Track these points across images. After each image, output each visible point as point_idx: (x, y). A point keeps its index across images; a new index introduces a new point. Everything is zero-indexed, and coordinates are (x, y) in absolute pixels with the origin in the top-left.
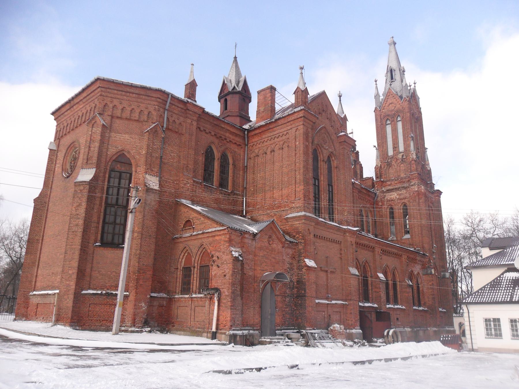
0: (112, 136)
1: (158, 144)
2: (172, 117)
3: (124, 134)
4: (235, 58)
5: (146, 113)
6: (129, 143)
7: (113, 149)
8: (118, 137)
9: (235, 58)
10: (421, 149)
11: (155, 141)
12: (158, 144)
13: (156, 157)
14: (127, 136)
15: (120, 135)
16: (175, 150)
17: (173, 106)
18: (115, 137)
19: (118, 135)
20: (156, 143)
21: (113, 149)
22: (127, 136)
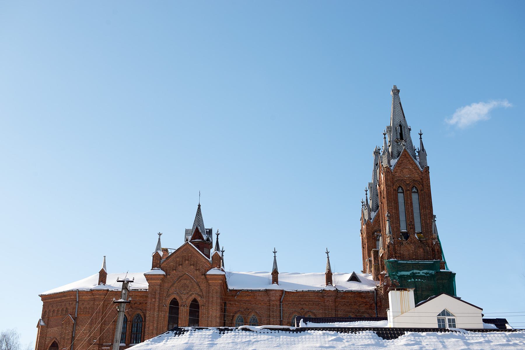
0: (49, 331)
1: (70, 329)
2: (83, 305)
3: (55, 327)
4: (199, 206)
5: (65, 309)
6: (56, 333)
7: (49, 340)
8: (52, 330)
9: (199, 206)
10: (423, 222)
11: (68, 327)
12: (70, 329)
13: (68, 339)
14: (56, 329)
15: (53, 328)
16: (88, 328)
17: (84, 297)
18: (50, 331)
19: (52, 329)
20: (68, 329)
21: (49, 340)
22: (56, 328)
